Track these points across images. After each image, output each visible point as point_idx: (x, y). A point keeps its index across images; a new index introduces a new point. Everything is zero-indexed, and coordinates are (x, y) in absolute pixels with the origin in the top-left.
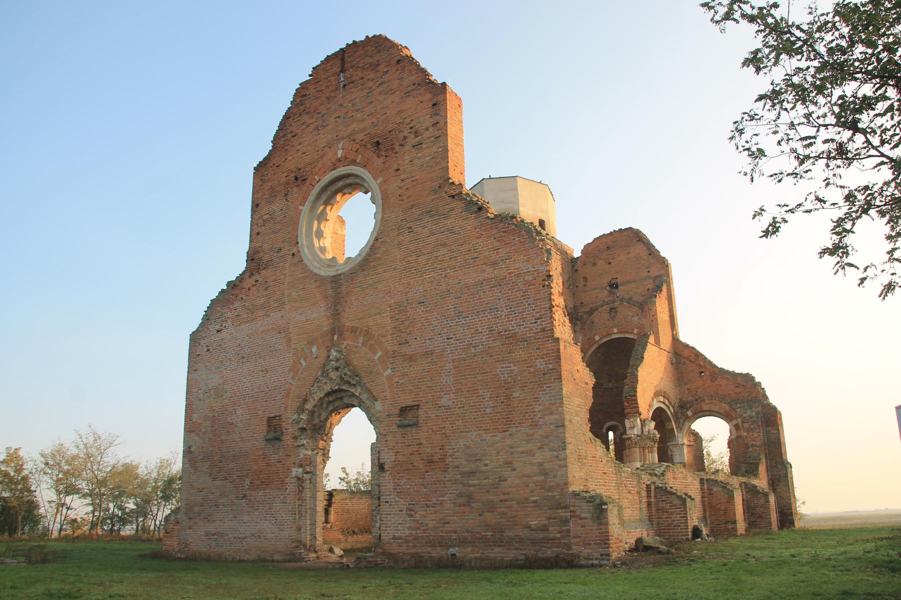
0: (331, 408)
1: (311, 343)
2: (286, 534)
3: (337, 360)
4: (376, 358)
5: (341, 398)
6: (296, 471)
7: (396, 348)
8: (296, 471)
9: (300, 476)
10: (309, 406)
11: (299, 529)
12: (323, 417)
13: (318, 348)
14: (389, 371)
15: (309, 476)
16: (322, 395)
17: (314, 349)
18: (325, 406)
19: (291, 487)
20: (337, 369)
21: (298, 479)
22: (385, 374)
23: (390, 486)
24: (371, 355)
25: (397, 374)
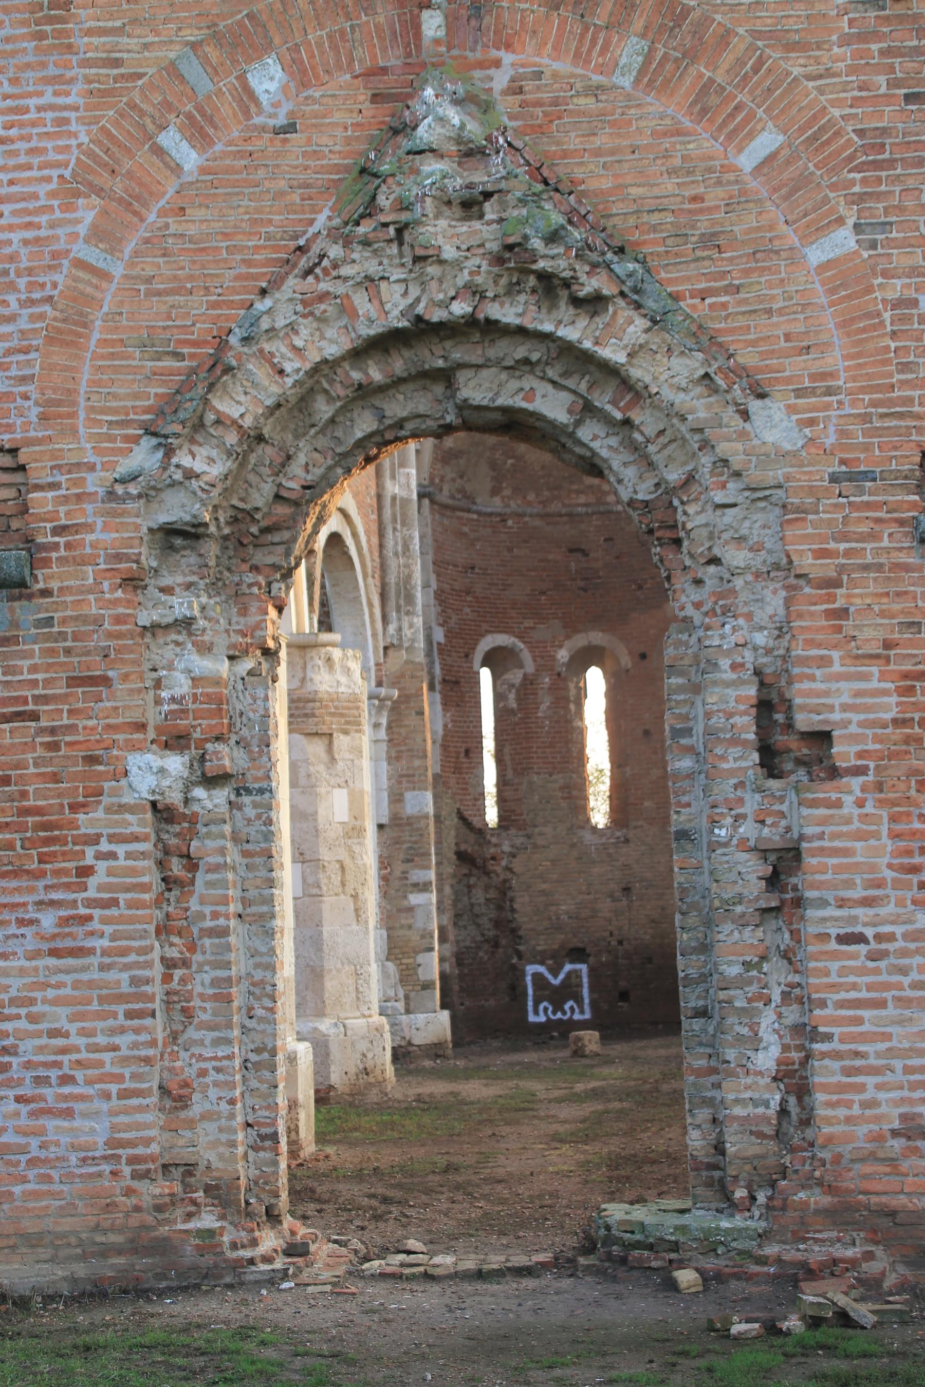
0: (364, 424)
1: (242, 42)
2: (94, 1129)
3: (471, 153)
4: (747, 160)
5: (446, 377)
6: (154, 772)
7: (889, 116)
8: (154, 772)
9: (175, 798)
10: (238, 404)
11: (175, 1097)
12: (296, 477)
13: (301, 75)
14: (843, 240)
15: (221, 796)
16: (332, 351)
17: (268, 80)
18: (324, 409)
19: (123, 861)
20: (471, 205)
21: (162, 812)
22: (816, 255)
23: (880, 853)
24: (704, 143)
25: (899, 258)
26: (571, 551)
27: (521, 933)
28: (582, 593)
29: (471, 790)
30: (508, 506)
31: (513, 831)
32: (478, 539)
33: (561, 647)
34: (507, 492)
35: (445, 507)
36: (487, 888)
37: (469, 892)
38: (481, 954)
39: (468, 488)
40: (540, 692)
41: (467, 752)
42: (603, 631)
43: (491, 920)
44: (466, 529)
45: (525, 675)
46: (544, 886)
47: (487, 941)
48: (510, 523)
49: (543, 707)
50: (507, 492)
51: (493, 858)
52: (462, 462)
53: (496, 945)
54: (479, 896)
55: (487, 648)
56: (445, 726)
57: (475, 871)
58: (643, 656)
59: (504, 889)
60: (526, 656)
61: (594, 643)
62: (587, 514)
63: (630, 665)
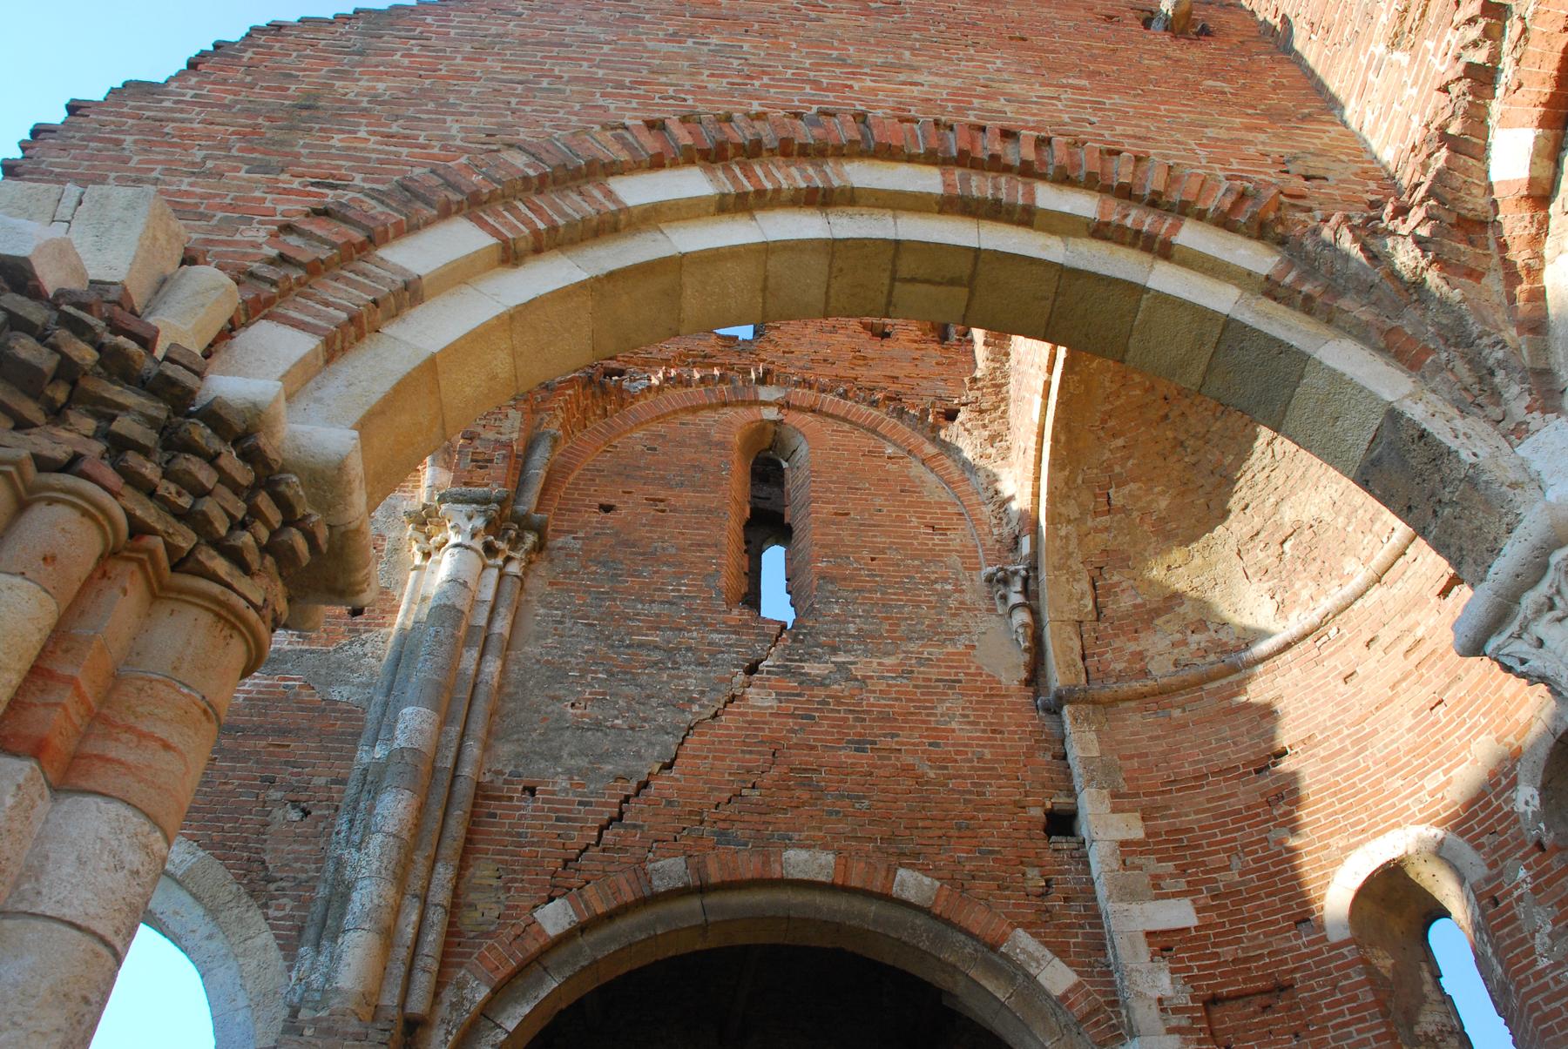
34: (1305, 594)
40: (1519, 910)
49: (1540, 941)
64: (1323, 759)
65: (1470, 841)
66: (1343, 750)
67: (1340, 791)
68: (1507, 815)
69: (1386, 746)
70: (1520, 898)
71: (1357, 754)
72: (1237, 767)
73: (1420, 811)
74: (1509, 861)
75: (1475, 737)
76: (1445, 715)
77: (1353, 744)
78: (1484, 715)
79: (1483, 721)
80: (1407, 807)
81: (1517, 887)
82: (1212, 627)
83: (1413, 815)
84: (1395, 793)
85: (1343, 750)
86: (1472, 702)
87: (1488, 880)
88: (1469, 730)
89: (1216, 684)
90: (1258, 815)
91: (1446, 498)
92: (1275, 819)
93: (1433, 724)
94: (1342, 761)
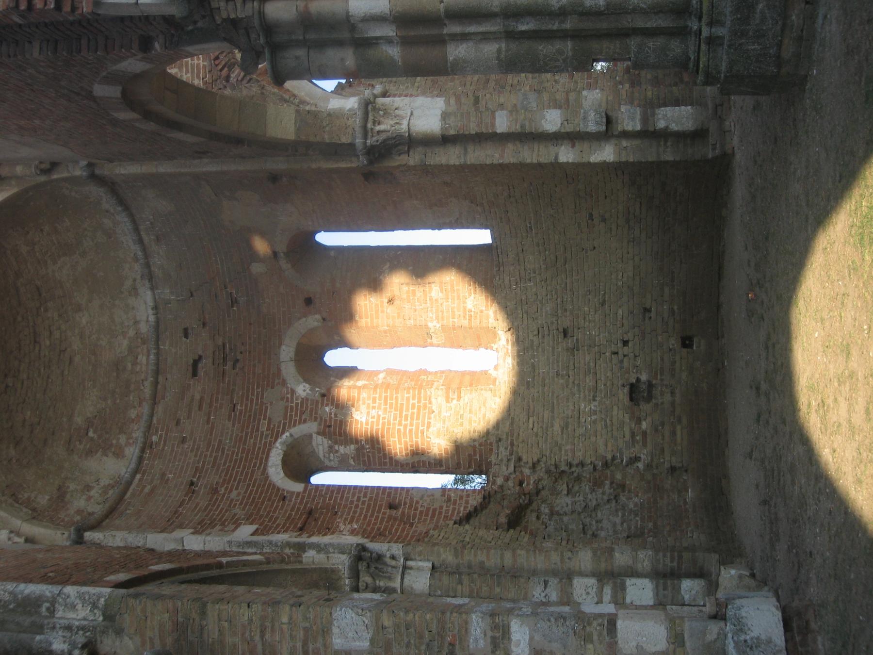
26: (195, 374)
27: (609, 457)
28: (238, 365)
29: (437, 505)
30: (137, 439)
31: (493, 459)
32: (163, 475)
33: (293, 392)
35: (110, 513)
36: (555, 492)
37: (558, 514)
38: (631, 506)
39: (105, 481)
41: (392, 507)
42: (280, 344)
43: (593, 491)
44: (148, 489)
45: (318, 433)
46: (557, 428)
47: (616, 498)
48: (155, 438)
50: (123, 439)
51: (521, 484)
52: (72, 486)
53: (623, 486)
54: (563, 502)
55: (282, 474)
56: (353, 532)
57: (534, 506)
58: (309, 301)
59: (557, 474)
60: (298, 430)
61: (292, 354)
62: (157, 354)
63: (318, 317)
64: (212, 467)
65: (299, 423)
66: (216, 458)
67: (234, 467)
68: (302, 403)
69: (231, 439)
70: (336, 415)
71: (223, 452)
72: (184, 500)
73: (271, 437)
74: (319, 412)
75: (262, 398)
76: (241, 406)
77: (217, 451)
78: (258, 388)
79: (260, 390)
80: (265, 443)
81: (331, 414)
82: (94, 484)
83: (271, 442)
84: (255, 444)
85: (216, 458)
86: (248, 391)
87: (320, 424)
88: (257, 399)
89: (131, 490)
90: (217, 499)
91: (325, 124)
92: (224, 494)
93: (241, 414)
94: (221, 460)
